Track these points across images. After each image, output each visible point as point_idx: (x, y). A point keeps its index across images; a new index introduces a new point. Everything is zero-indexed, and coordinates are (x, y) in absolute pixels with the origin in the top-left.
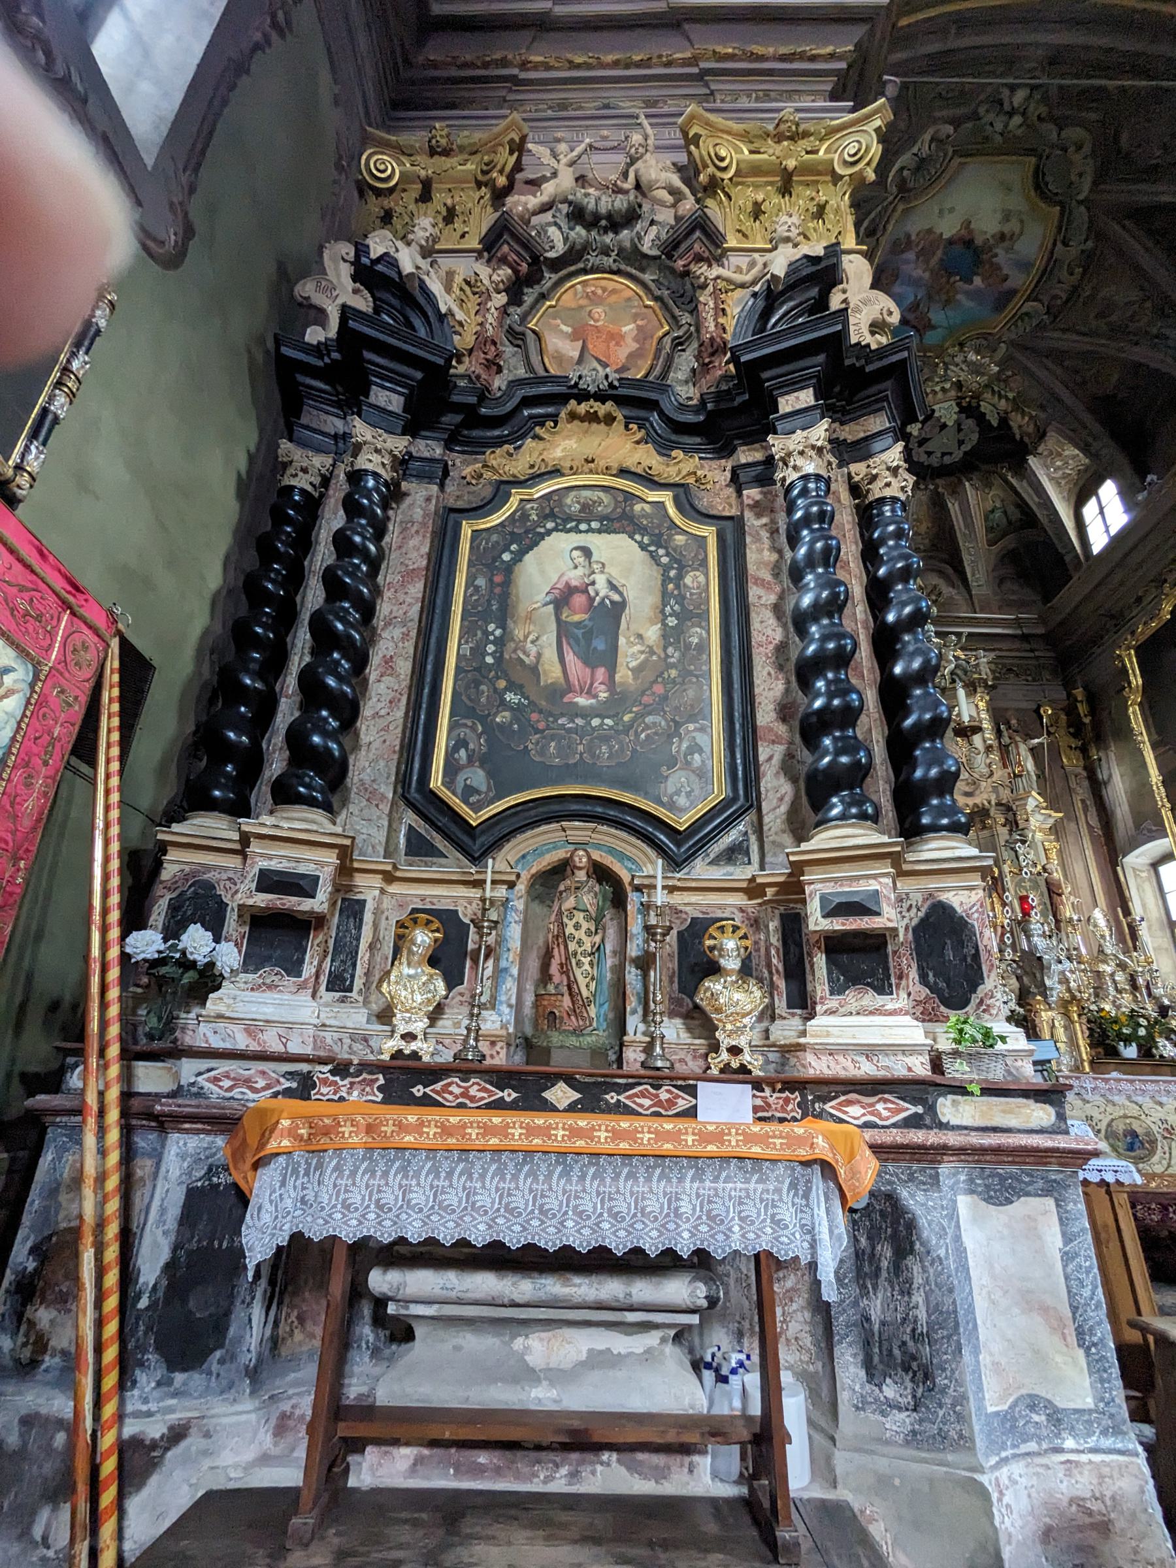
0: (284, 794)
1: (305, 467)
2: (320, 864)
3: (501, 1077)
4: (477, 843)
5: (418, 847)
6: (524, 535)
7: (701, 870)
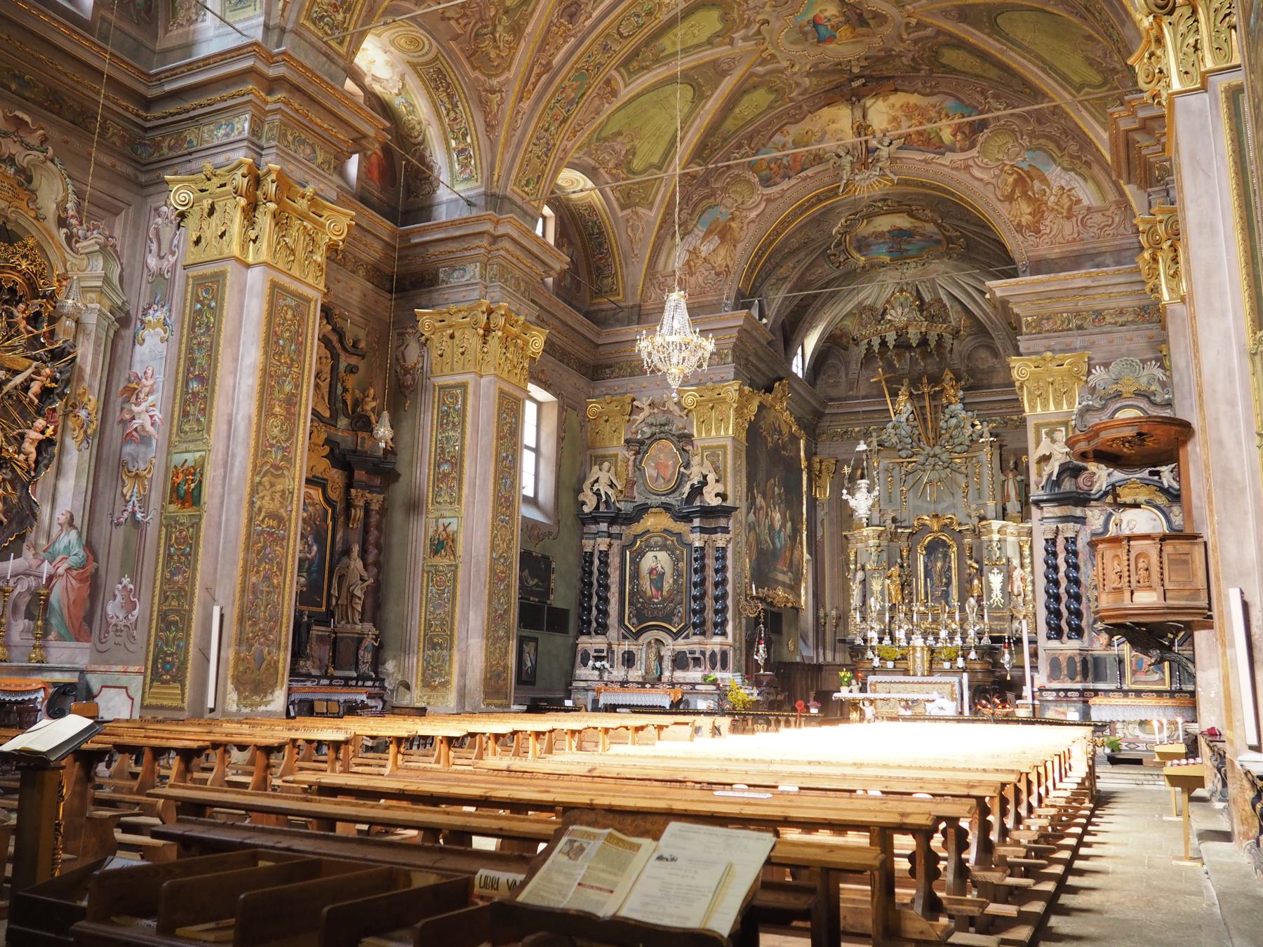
0: (597, 634)
1: (588, 545)
2: (604, 647)
3: (638, 683)
4: (637, 636)
5: (625, 637)
6: (641, 553)
7: (680, 641)
